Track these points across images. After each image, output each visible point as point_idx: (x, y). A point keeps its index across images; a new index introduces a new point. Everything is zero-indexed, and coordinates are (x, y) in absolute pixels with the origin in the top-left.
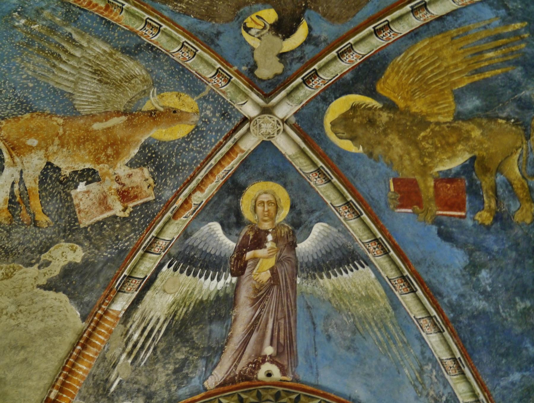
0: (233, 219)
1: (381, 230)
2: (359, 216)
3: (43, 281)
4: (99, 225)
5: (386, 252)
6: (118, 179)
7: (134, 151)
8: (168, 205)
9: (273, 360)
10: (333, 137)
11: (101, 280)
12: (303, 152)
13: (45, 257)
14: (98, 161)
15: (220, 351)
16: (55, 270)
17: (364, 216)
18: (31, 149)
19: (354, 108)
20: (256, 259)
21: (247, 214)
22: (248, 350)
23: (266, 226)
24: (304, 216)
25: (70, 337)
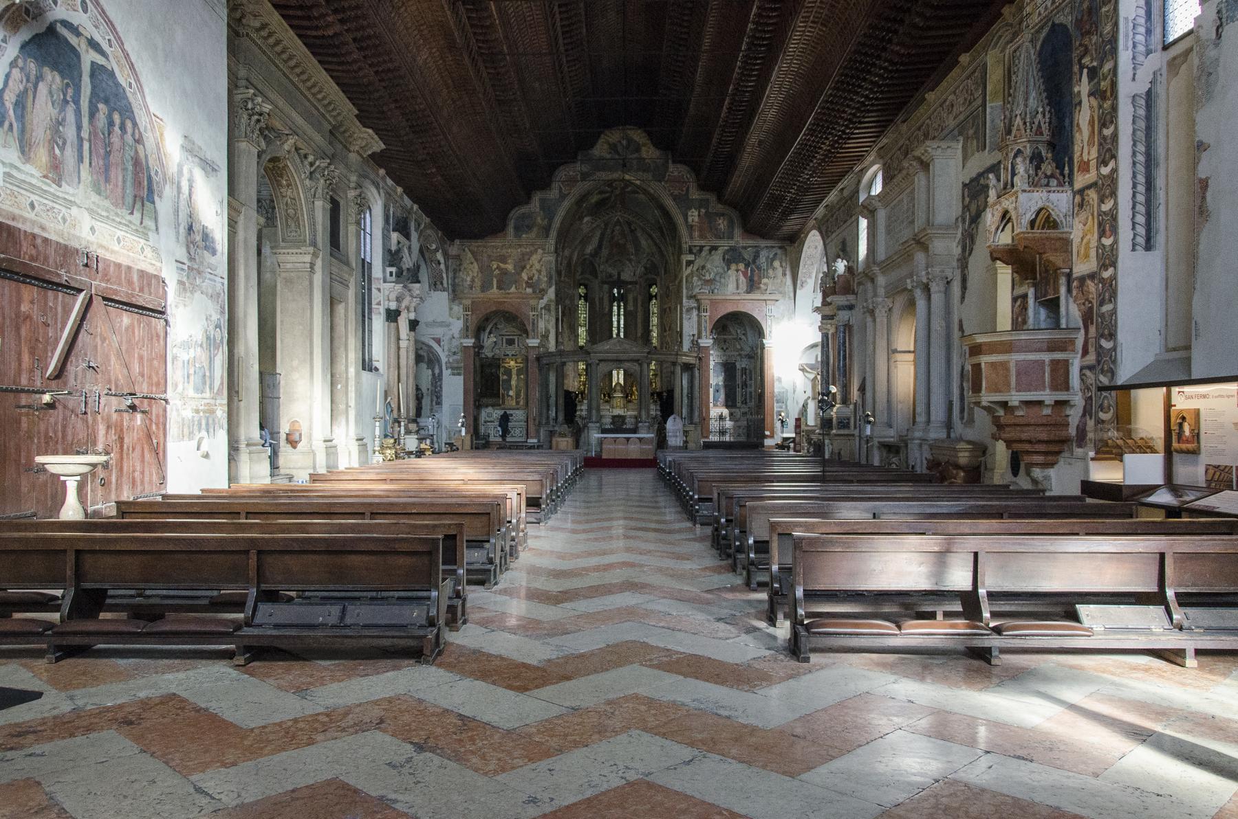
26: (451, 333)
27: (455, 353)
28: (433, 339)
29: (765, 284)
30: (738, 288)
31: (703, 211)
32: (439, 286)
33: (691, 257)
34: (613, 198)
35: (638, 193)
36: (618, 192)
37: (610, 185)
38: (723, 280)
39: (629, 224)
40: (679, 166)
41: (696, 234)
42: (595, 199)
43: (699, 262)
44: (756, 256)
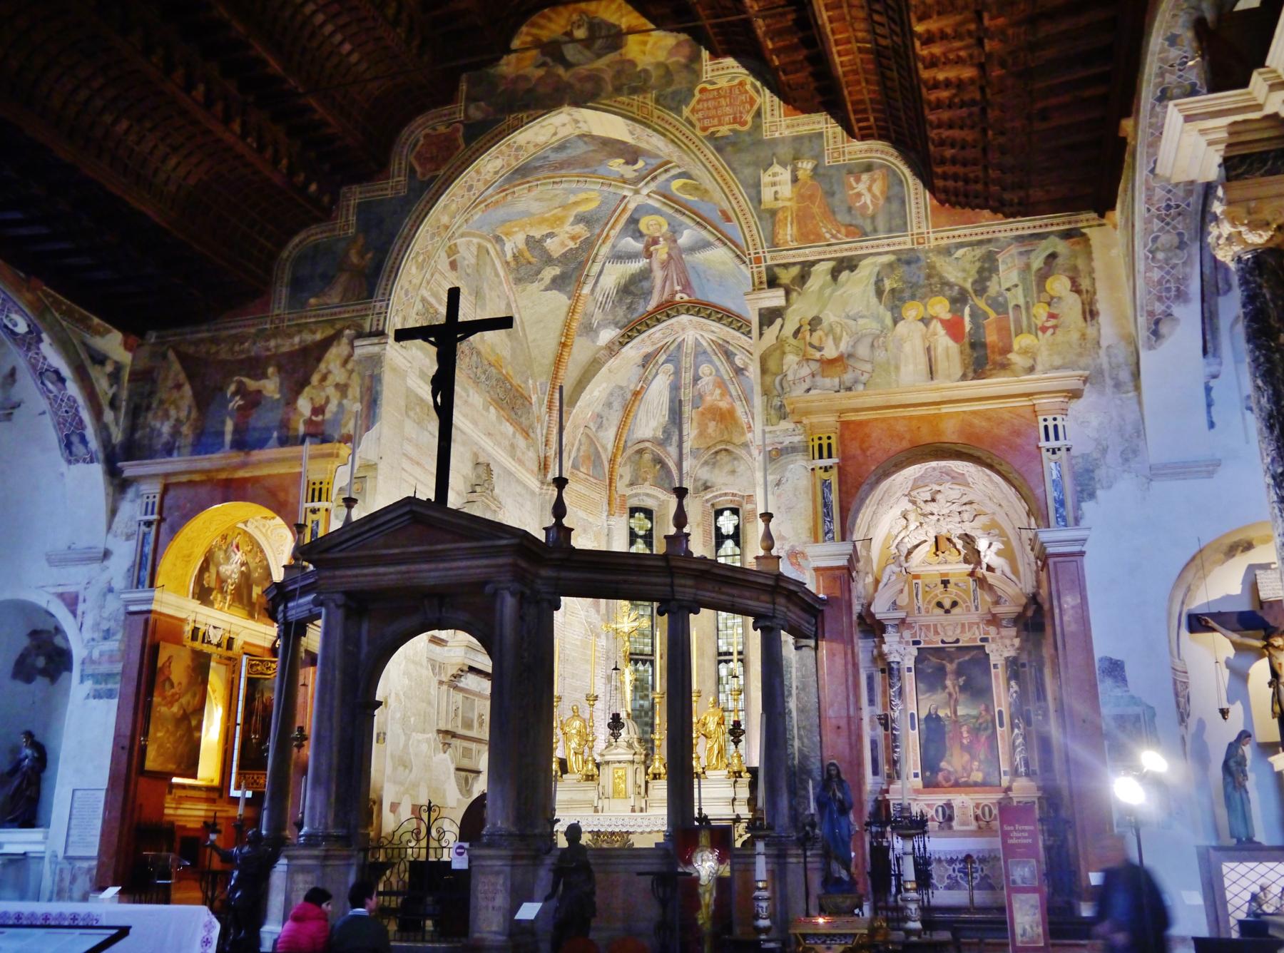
0: (638, 234)
1: (720, 232)
2: (706, 228)
3: (543, 288)
4: (564, 255)
5: (726, 244)
6: (567, 232)
7: (572, 219)
8: (599, 236)
9: (681, 292)
10: (679, 194)
11: (574, 278)
12: (665, 203)
13: (540, 276)
14: (553, 228)
15: (651, 293)
16: (547, 281)
17: (709, 227)
18: (516, 232)
19: (685, 184)
20: (657, 250)
21: (644, 230)
22: (666, 289)
23: (657, 234)
24: (677, 228)
25: (565, 309)
26: (105, 577)
27: (107, 635)
28: (61, 596)
29: (1025, 352)
30: (932, 373)
31: (806, 166)
32: (79, 449)
33: (775, 298)
34: (658, 275)
35: (706, 245)
36: (661, 251)
37: (638, 235)
38: (881, 355)
39: (729, 356)
40: (730, 61)
41: (788, 232)
42: (613, 276)
43: (801, 310)
44: (988, 268)
